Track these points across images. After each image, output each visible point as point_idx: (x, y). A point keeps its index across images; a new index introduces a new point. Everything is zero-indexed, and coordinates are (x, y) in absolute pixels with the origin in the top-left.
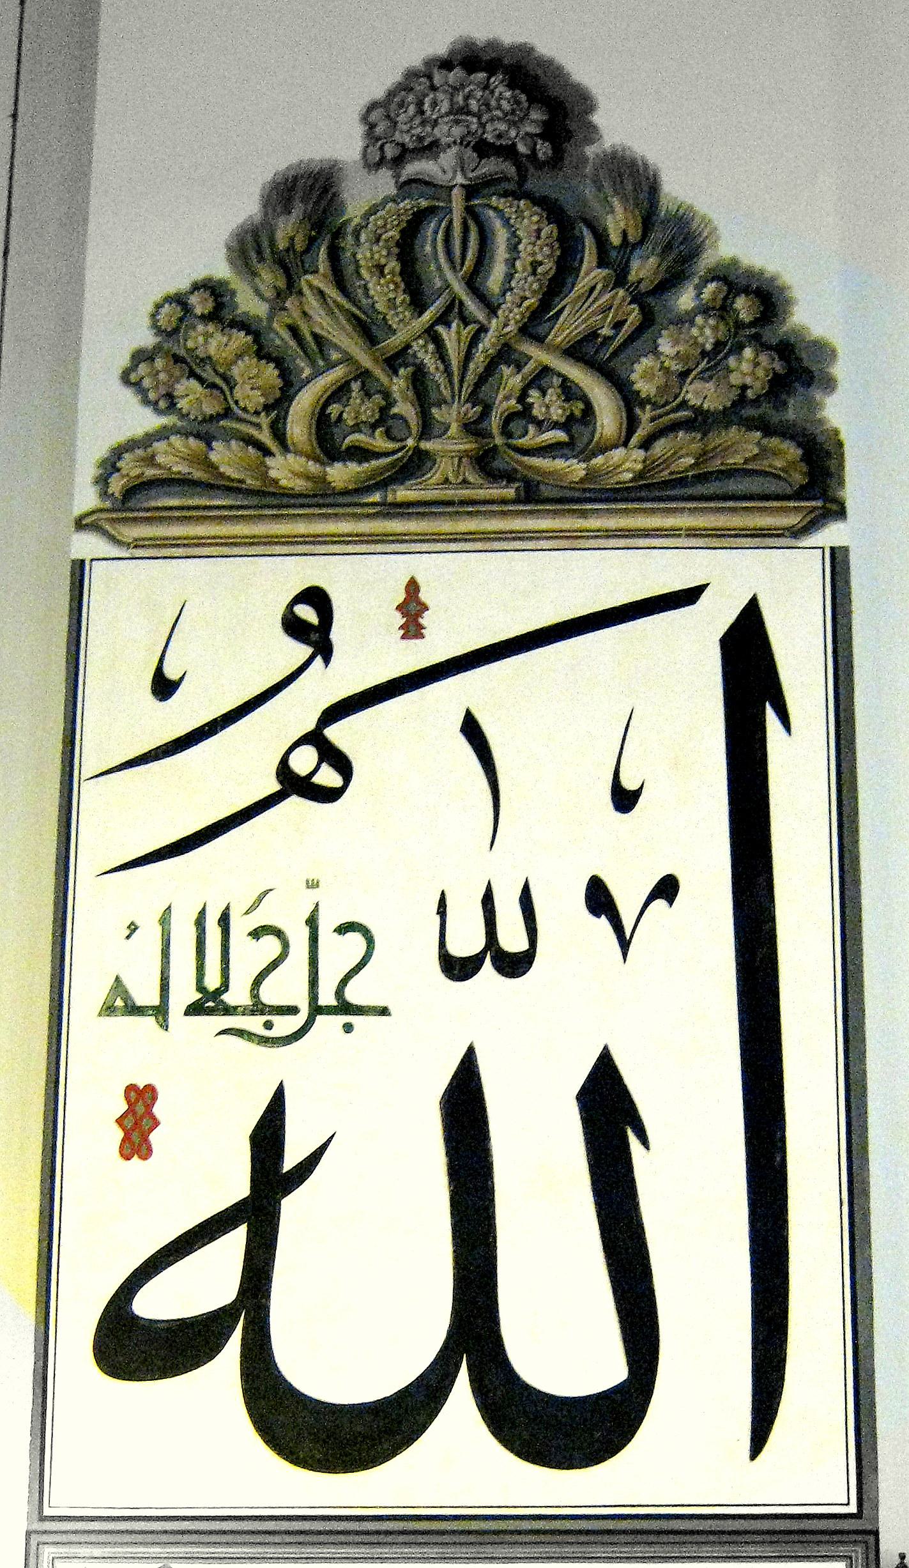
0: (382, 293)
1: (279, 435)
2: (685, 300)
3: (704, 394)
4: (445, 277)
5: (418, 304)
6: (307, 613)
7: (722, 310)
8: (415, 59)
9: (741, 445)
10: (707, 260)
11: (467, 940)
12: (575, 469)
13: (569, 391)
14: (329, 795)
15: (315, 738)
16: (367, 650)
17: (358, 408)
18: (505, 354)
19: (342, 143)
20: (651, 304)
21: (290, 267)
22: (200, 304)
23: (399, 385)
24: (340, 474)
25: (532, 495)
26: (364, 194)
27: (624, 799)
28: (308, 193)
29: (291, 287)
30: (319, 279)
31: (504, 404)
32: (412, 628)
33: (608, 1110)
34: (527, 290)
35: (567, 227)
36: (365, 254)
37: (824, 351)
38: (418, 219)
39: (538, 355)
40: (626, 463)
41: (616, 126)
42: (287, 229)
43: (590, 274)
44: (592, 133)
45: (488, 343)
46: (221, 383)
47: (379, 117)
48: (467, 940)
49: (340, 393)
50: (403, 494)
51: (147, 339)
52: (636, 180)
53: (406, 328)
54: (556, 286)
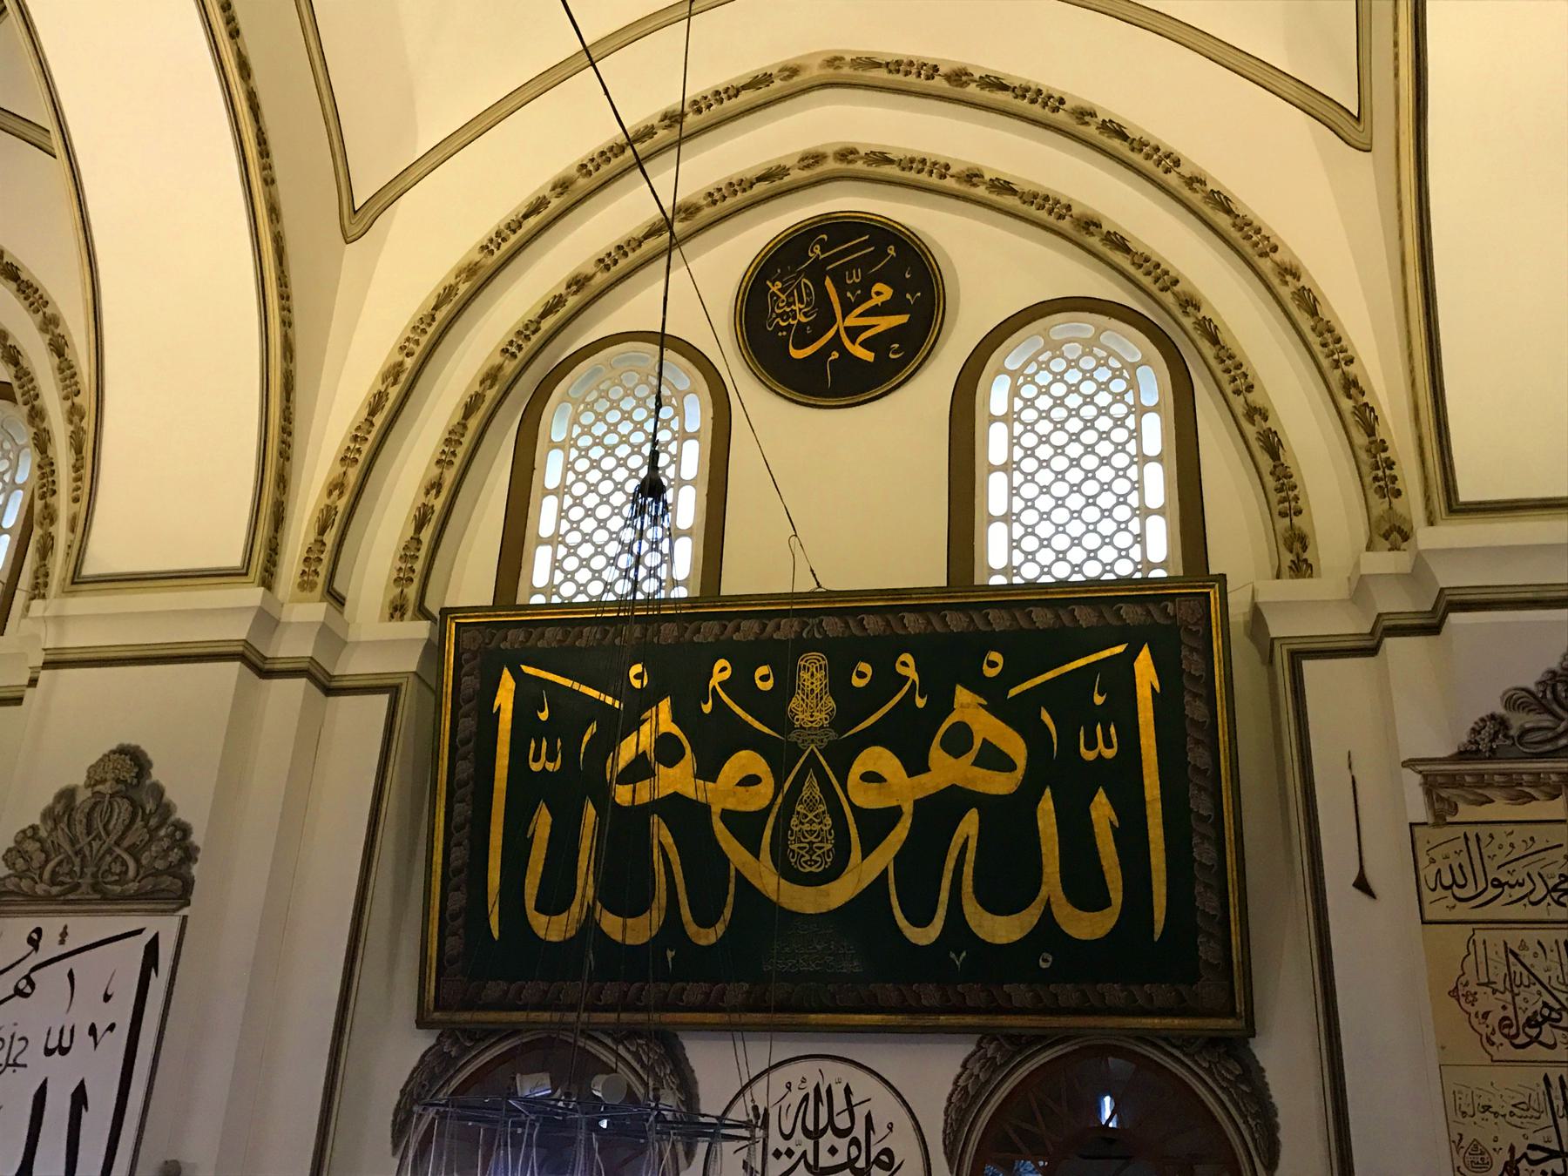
0: (80, 829)
1: (41, 877)
2: (162, 833)
3: (160, 865)
4: (98, 824)
5: (88, 834)
6: (35, 936)
7: (171, 836)
8: (106, 751)
9: (166, 881)
10: (172, 819)
11: (53, 1044)
12: (118, 889)
13: (124, 863)
14: (27, 995)
15: (27, 977)
16: (49, 948)
17: (65, 868)
18: (110, 851)
19: (80, 779)
20: (153, 832)
21: (56, 821)
22: (29, 833)
23: (77, 861)
24: (55, 890)
25: (107, 898)
26: (83, 796)
27: (107, 998)
28: (67, 795)
29: (55, 829)
30: (64, 825)
31: (104, 867)
32: (62, 942)
33: (79, 1098)
34: (120, 828)
35: (136, 806)
36: (79, 816)
37: (197, 849)
38: (96, 804)
39: (118, 851)
40: (133, 887)
41: (157, 774)
42: (59, 809)
43: (139, 823)
44: (150, 775)
45: (105, 847)
46: (28, 859)
47: (93, 769)
48: (51, 1045)
49: (60, 864)
50: (71, 897)
51: (12, 844)
52: (158, 791)
53: (84, 841)
54: (128, 827)
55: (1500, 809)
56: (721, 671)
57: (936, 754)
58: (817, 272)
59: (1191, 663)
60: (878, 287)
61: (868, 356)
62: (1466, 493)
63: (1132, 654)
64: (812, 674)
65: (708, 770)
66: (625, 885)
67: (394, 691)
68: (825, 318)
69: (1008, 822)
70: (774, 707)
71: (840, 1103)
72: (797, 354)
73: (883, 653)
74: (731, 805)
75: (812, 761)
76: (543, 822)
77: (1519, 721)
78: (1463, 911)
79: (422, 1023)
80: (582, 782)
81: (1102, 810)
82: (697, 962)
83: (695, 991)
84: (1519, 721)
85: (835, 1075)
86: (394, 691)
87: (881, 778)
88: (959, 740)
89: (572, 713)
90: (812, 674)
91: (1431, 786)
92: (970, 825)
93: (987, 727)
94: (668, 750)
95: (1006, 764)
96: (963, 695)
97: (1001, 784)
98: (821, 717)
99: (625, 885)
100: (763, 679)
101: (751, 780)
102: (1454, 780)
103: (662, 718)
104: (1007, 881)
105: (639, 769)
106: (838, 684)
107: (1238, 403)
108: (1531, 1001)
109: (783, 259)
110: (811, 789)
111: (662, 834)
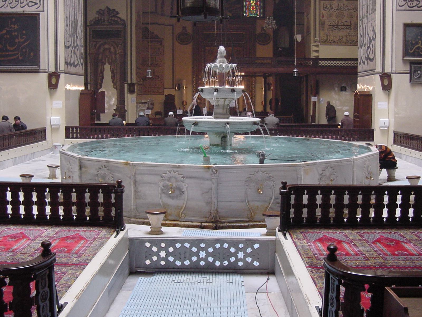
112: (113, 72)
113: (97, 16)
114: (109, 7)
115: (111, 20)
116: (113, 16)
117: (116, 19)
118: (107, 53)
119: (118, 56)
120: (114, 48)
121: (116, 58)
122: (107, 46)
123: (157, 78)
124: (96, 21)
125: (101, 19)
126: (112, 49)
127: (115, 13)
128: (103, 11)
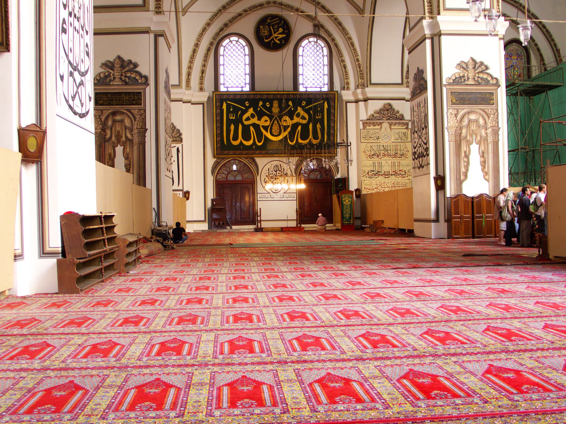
9: (178, 139)
55: (372, 127)
56: (261, 103)
57: (295, 117)
58: (269, 25)
59: (332, 104)
60: (280, 29)
61: (278, 42)
62: (372, 82)
63: (324, 103)
64: (276, 104)
65: (259, 119)
66: (247, 137)
67: (203, 104)
68: (271, 35)
69: (305, 127)
70: (270, 109)
71: (279, 167)
72: (266, 41)
73: (287, 100)
74: (263, 125)
75: (276, 118)
76: (232, 127)
77: (375, 115)
78: (366, 141)
79: (214, 157)
80: (238, 121)
81: (318, 126)
82: (258, 148)
83: (258, 152)
84: (375, 115)
85: (278, 163)
86: (203, 104)
87: (287, 121)
88: (298, 115)
89: (236, 110)
90: (276, 104)
91: (363, 124)
92: (300, 128)
93: (303, 113)
94: (253, 116)
95: (305, 119)
96: (299, 108)
97: (304, 122)
98: (277, 111)
99: (247, 137)
100: (268, 105)
101: (266, 121)
102: (366, 123)
103: (251, 111)
104: (304, 136)
105: (248, 119)
106: (280, 106)
107: (340, 59)
108: (373, 153)
109: (263, 21)
110: (276, 122)
111: (252, 129)
112: (482, 155)
113: (458, 71)
114: (475, 58)
115: (478, 77)
116: (481, 72)
117: (485, 76)
118: (473, 127)
119: (489, 131)
120: (484, 119)
121: (486, 134)
122: (473, 117)
123: (404, 173)
124: (456, 78)
125: (464, 76)
126: (481, 122)
127: (483, 67)
128: (467, 64)
